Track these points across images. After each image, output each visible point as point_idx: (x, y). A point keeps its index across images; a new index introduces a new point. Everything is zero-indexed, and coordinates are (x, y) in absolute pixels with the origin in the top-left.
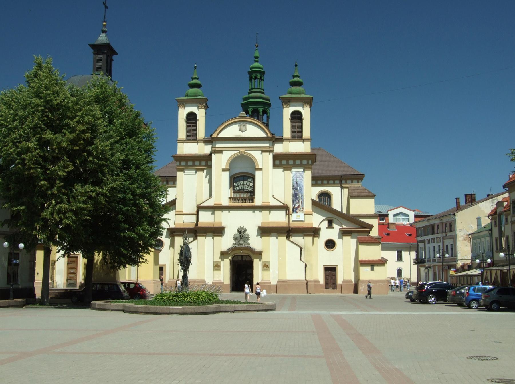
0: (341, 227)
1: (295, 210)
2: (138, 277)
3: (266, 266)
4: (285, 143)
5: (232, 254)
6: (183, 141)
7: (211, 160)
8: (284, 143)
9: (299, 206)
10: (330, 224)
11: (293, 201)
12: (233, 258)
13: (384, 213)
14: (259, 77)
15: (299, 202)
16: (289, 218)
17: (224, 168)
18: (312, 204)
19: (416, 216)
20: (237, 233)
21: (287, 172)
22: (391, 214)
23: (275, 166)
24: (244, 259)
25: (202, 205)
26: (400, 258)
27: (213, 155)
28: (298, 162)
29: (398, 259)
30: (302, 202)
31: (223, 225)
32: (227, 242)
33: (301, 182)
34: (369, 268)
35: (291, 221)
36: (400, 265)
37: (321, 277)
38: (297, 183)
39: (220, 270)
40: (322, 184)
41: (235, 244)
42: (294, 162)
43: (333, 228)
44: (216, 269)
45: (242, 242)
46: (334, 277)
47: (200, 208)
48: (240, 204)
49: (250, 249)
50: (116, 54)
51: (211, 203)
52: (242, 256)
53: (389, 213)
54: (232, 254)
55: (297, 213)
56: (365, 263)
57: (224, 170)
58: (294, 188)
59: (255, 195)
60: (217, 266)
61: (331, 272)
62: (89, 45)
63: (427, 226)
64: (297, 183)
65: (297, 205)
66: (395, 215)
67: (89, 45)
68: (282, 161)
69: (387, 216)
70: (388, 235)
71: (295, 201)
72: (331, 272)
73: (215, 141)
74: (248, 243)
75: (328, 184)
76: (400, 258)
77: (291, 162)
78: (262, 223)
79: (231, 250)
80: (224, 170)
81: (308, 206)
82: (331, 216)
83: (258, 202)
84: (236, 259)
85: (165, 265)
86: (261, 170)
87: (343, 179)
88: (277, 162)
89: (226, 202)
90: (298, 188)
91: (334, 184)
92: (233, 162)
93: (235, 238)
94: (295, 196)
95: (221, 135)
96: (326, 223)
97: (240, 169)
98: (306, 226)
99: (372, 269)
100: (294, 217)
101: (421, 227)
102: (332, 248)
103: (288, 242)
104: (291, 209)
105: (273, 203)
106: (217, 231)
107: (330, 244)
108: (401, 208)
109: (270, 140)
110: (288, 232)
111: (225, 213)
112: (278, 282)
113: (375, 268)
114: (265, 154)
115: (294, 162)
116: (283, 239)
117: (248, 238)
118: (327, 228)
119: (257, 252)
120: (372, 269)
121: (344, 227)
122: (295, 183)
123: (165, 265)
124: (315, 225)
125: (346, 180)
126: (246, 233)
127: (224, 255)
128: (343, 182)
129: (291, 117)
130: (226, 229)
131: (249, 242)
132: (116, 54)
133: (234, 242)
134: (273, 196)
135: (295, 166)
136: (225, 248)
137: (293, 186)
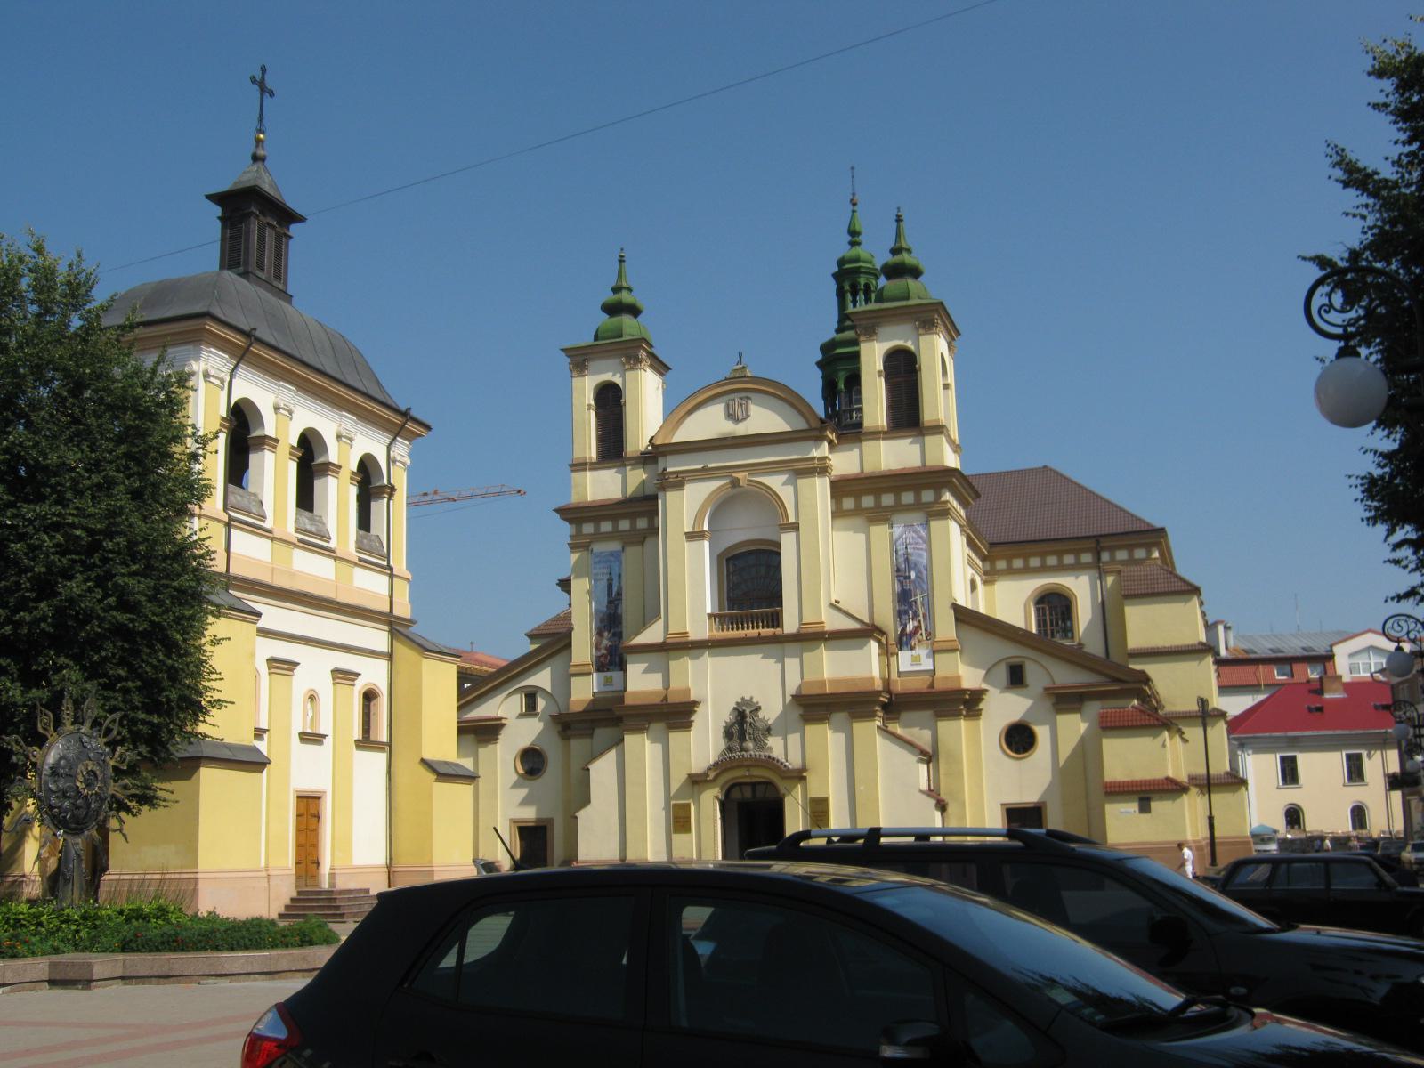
0: (1048, 683)
1: (904, 640)
2: (391, 859)
4: (868, 446)
5: (723, 779)
8: (864, 444)
9: (917, 629)
11: (900, 614)
12: (728, 793)
13: (1321, 650)
15: (915, 615)
16: (889, 665)
17: (688, 529)
18: (957, 620)
21: (880, 532)
22: (1342, 655)
23: (838, 513)
24: (759, 794)
26: (1355, 772)
28: (908, 498)
29: (1350, 778)
30: (924, 616)
32: (703, 745)
33: (920, 556)
34: (1132, 807)
35: (894, 676)
36: (1356, 794)
38: (907, 561)
39: (688, 830)
40: (1043, 570)
41: (730, 749)
42: (898, 499)
43: (1027, 686)
45: (750, 745)
49: (771, 763)
50: (298, 219)
52: (754, 785)
53: (1336, 649)
54: (723, 779)
55: (912, 648)
56: (1120, 791)
58: (900, 574)
59: (781, 606)
60: (679, 820)
62: (209, 197)
64: (907, 561)
65: (911, 626)
66: (1351, 655)
67: (209, 197)
68: (863, 498)
69: (1329, 657)
70: (1320, 709)
71: (906, 613)
73: (664, 454)
75: (1061, 569)
76: (1355, 772)
77: (888, 500)
79: (720, 767)
81: (946, 627)
82: (1011, 651)
83: (790, 624)
84: (736, 794)
85: (551, 821)
86: (795, 527)
87: (1103, 549)
88: (848, 503)
90: (913, 575)
91: (1077, 568)
92: (720, 508)
93: (728, 734)
94: (904, 600)
95: (681, 436)
97: (743, 530)
98: (939, 686)
99: (1145, 808)
100: (905, 661)
104: (892, 641)
106: (675, 714)
108: (1370, 635)
109: (819, 438)
110: (890, 704)
113: (1154, 805)
114: (802, 482)
115: (898, 499)
116: (868, 731)
120: (1145, 808)
122: (902, 559)
123: (551, 821)
125: (1112, 549)
128: (1105, 556)
129: (884, 368)
130: (699, 710)
132: (298, 219)
133: (722, 744)
134: (835, 606)
135: (899, 508)
137: (898, 570)
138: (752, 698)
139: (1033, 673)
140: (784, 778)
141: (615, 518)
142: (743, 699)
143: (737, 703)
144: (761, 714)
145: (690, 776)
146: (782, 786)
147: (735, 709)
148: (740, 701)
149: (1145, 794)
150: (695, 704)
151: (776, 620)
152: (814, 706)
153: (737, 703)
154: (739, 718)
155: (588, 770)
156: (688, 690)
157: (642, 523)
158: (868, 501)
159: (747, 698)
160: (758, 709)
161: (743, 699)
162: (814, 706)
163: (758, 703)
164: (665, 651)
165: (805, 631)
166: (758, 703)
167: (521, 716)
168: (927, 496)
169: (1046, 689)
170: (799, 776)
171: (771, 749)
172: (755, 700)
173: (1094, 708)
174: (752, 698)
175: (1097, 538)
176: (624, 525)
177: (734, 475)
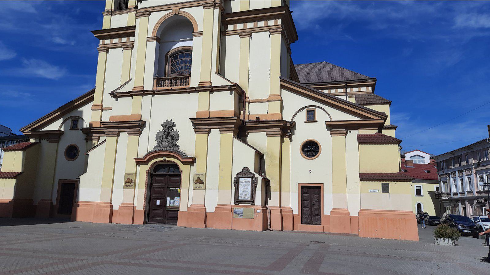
0: (330, 120)
3: (200, 182)
6: (111, 13)
10: (311, 117)
19: (431, 158)
20: (161, 129)
25: (118, 91)
28: (261, 24)
36: (419, 199)
37: (293, 203)
41: (158, 146)
43: (317, 122)
46: (316, 204)
47: (115, 95)
48: (170, 88)
51: (128, 88)
53: (405, 155)
57: (149, 39)
59: (190, 74)
60: (130, 182)
61: (311, 194)
63: (451, 158)
72: (311, 194)
77: (250, 25)
79: (151, 156)
80: (149, 39)
86: (200, 34)
88: (231, 27)
89: (149, 85)
96: (303, 115)
98: (270, 119)
99: (385, 189)
101: (442, 161)
102: (313, 155)
103: (237, 142)
105: (217, 81)
107: (311, 149)
112: (216, 208)
118: (305, 122)
119: (188, 158)
120: (385, 189)
121: (333, 120)
124: (287, 118)
126: (174, 128)
127: (139, 162)
128: (349, 90)
136: (142, 154)
138: (171, 120)
139: (319, 113)
140: (184, 163)
141: (120, 36)
142: (167, 120)
143: (164, 123)
146: (182, 167)
149: (385, 179)
150: (145, 122)
151: (187, 83)
152: (203, 124)
153: (164, 123)
154: (163, 131)
155: (88, 155)
157: (132, 39)
158: (240, 26)
159: (169, 120)
160: (175, 126)
161: (167, 120)
162: (203, 124)
163: (174, 123)
165: (200, 86)
166: (174, 123)
167: (70, 129)
168: (271, 23)
169: (326, 122)
170: (192, 162)
172: (173, 122)
173: (353, 135)
174: (171, 120)
175: (346, 82)
176: (124, 40)
177: (173, 8)
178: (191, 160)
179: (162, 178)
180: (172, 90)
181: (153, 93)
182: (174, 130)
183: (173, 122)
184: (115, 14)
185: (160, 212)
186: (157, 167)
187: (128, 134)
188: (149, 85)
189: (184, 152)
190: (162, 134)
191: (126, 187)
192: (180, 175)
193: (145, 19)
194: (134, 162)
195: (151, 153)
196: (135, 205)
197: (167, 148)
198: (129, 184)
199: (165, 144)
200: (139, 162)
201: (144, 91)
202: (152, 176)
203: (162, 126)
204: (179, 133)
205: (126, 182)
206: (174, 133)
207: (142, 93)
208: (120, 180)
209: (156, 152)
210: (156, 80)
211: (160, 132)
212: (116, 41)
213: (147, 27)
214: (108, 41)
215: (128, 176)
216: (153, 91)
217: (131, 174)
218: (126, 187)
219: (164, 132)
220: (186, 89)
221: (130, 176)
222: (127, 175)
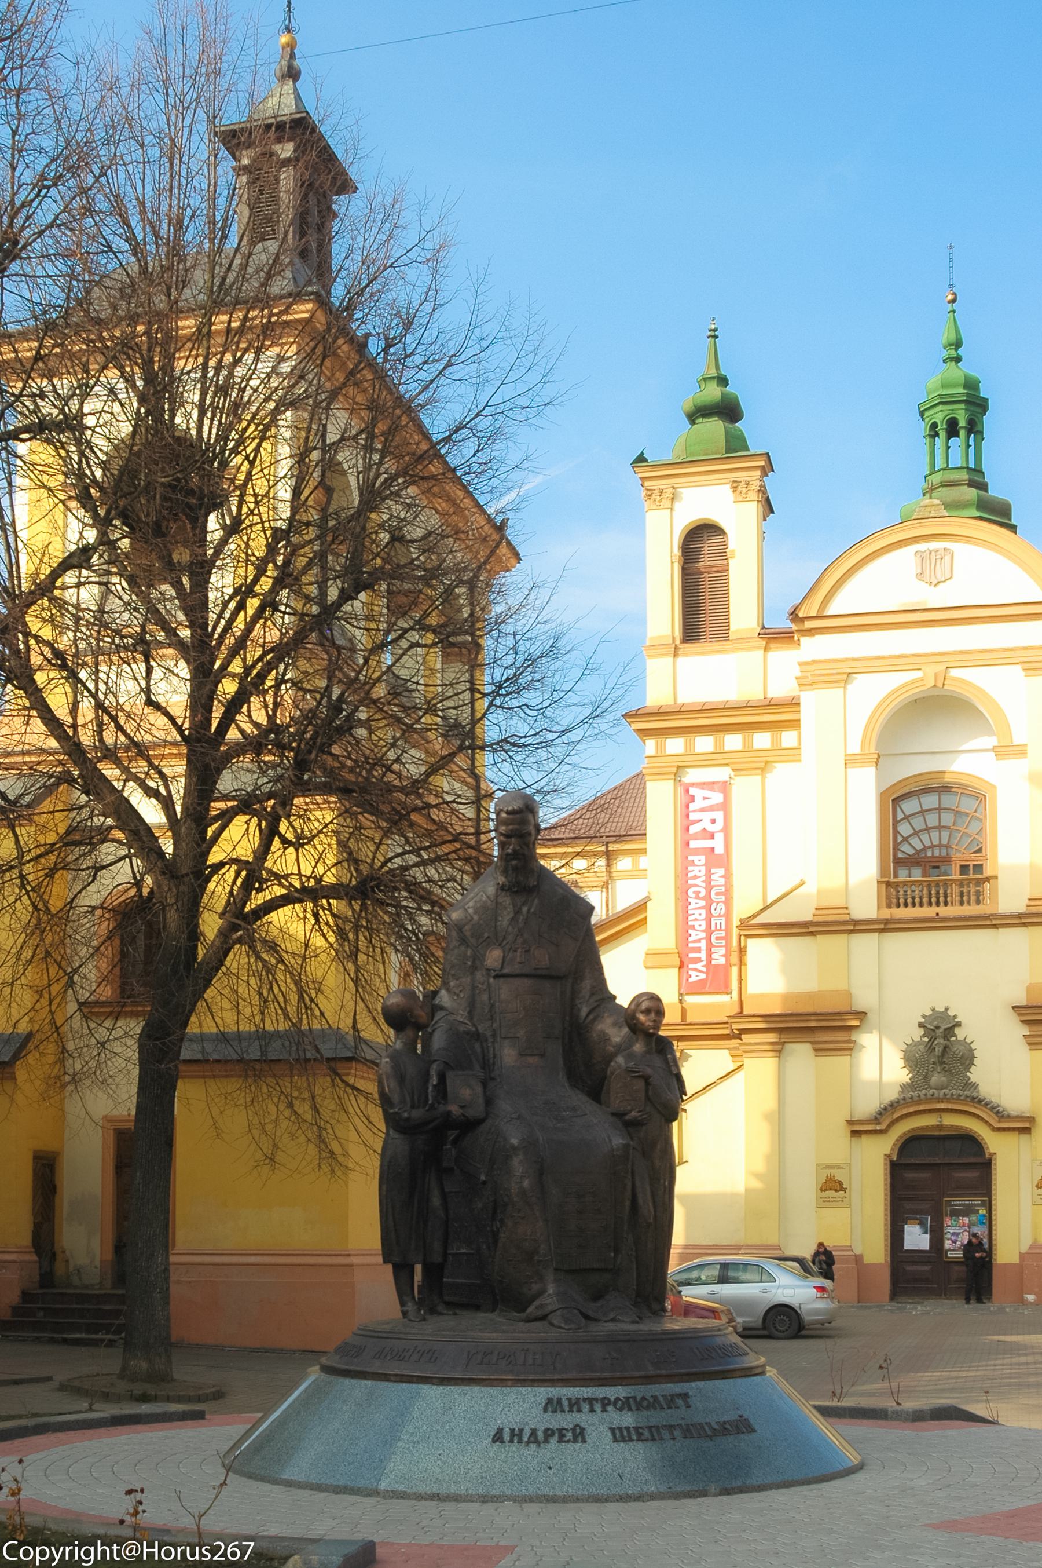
7: (795, 724)
14: (962, 423)
17: (855, 748)
20: (917, 1034)
27: (807, 699)
31: (859, 1005)
44: (826, 1200)
57: (850, 761)
60: (832, 1186)
74: (969, 1085)
78: (1030, 989)
80: (850, 761)
89: (866, 905)
111: (865, 944)
117: (968, 1059)
119: (1009, 1117)
126: (957, 1031)
127: (857, 1130)
131: (975, 1075)
136: (868, 1106)
138: (947, 1009)
142: (933, 1010)
143: (924, 1017)
144: (960, 1033)
145: (850, 1122)
146: (994, 1143)
147: (921, 1025)
148: (929, 1013)
150: (861, 1015)
153: (924, 1017)
154: (926, 1039)
156: (849, 995)
157: (762, 740)
161: (933, 1010)
163: (955, 1017)
164: (812, 934)
165: (1034, 910)
170: (1023, 1126)
171: (975, 1086)
174: (947, 1009)
176: (733, 741)
178: (1027, 1125)
179: (925, 1175)
180: (938, 918)
181: (885, 926)
182: (956, 1036)
183: (951, 1013)
184: (686, 654)
185: (926, 1268)
186: (910, 1143)
187: (816, 1050)
188: (866, 905)
189: (995, 1100)
190: (922, 1047)
191: (823, 1203)
192: (984, 1166)
193: (832, 695)
194: (845, 1131)
195: (893, 1106)
196: (858, 1251)
197: (947, 1091)
198: (831, 1193)
199: (935, 1079)
200: (857, 1130)
201: (856, 922)
202: (899, 1169)
203: (921, 1025)
204: (973, 1046)
205: (823, 1189)
206: (962, 1048)
207: (851, 928)
208: (805, 1187)
209: (913, 1101)
210: (884, 886)
211: (915, 1044)
212: (704, 743)
213: (839, 723)
214: (675, 745)
215: (828, 1172)
216: (887, 922)
217: (839, 1167)
218: (823, 1203)
219: (930, 1048)
220: (988, 917)
221: (833, 1172)
222: (820, 1167)
